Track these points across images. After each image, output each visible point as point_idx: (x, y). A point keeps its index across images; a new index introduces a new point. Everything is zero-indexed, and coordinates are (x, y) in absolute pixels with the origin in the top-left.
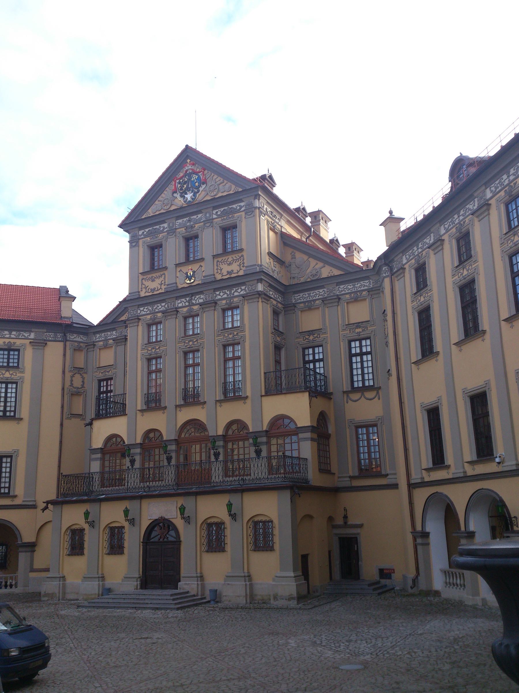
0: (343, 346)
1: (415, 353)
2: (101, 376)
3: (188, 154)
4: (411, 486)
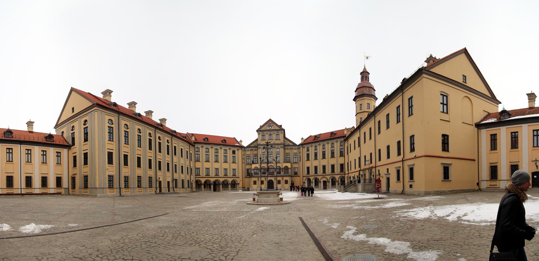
1: (306, 159)
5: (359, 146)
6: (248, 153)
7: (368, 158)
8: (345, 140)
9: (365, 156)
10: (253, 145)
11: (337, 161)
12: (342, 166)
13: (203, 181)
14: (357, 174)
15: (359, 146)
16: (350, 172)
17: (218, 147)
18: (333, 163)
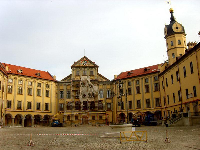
0: (106, 92)
2: (60, 91)
3: (85, 57)
4: (117, 112)
5: (178, 79)
6: (61, 88)
7: (191, 91)
8: (160, 76)
9: (187, 90)
10: (66, 81)
11: (152, 95)
12: (158, 100)
13: (14, 115)
14: (178, 108)
15: (178, 79)
16: (168, 106)
17: (32, 80)
18: (148, 98)
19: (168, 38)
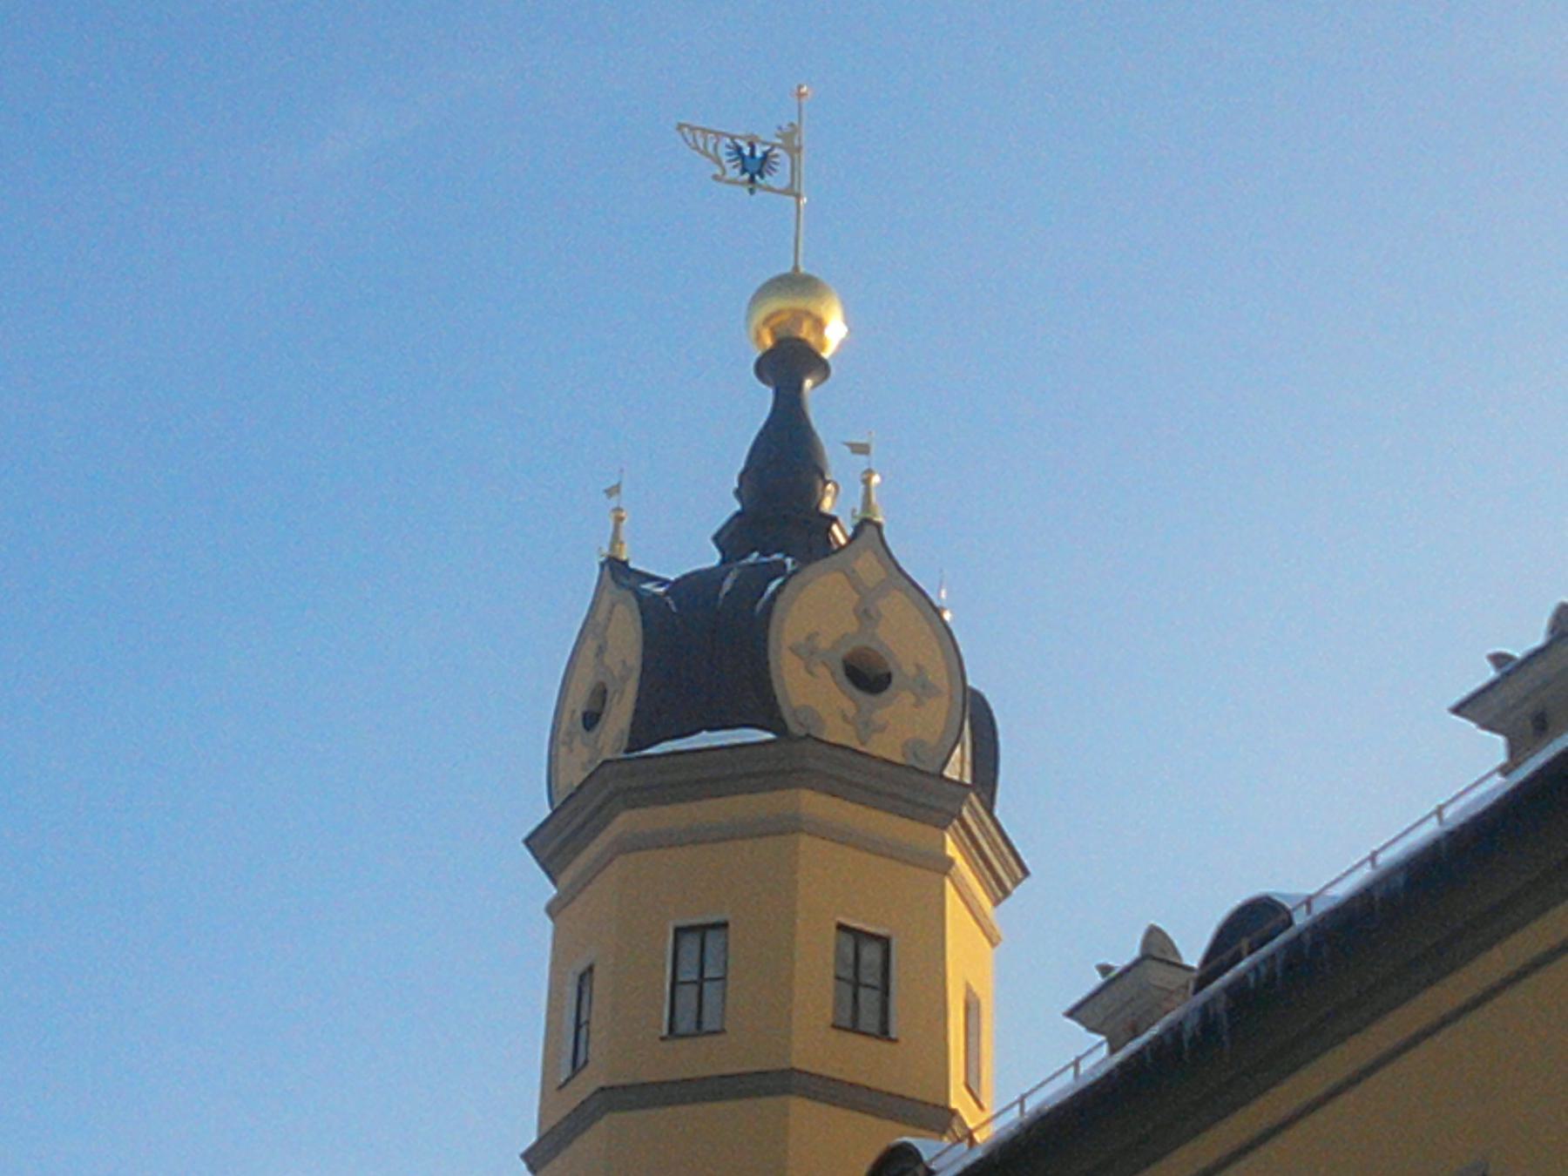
19: (625, 847)
